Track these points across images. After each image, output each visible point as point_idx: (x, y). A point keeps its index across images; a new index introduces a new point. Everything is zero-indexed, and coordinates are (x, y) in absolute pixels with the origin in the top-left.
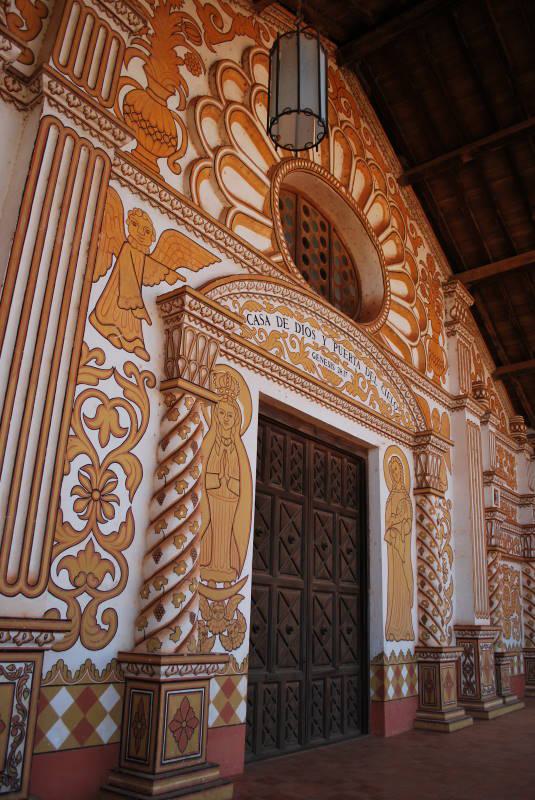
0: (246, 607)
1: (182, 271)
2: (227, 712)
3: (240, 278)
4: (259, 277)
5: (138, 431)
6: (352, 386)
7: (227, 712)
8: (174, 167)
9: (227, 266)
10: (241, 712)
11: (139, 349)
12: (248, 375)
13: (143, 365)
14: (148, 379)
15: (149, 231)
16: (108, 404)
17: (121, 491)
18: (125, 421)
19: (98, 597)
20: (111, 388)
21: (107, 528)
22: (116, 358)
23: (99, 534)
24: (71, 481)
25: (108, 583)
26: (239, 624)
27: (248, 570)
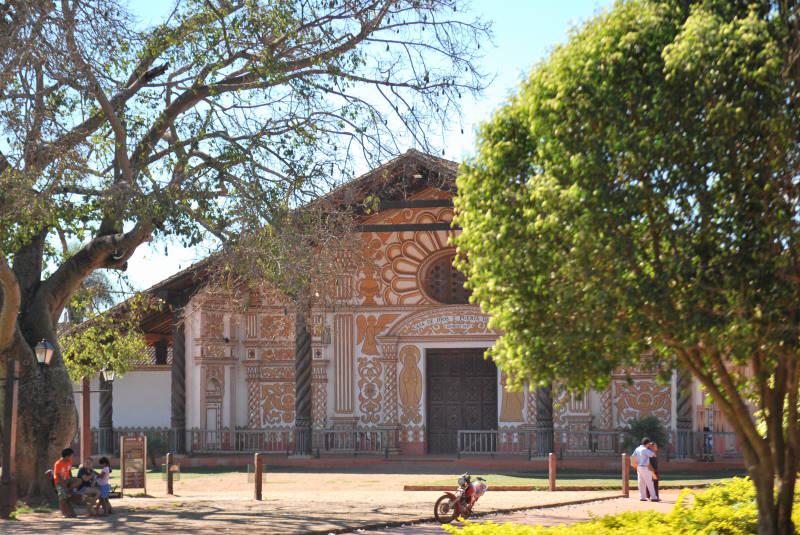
0: (422, 411)
1: (388, 325)
2: (416, 439)
3: (411, 315)
4: (418, 312)
5: (379, 374)
6: (475, 329)
7: (416, 439)
8: (379, 296)
9: (404, 314)
10: (422, 439)
11: (378, 354)
12: (416, 344)
13: (377, 357)
14: (380, 359)
15: (375, 320)
16: (370, 370)
17: (377, 389)
18: (375, 372)
19: (374, 413)
20: (370, 366)
21: (375, 397)
22: (370, 358)
23: (374, 400)
24: (363, 389)
25: (376, 409)
26: (420, 416)
27: (422, 401)
